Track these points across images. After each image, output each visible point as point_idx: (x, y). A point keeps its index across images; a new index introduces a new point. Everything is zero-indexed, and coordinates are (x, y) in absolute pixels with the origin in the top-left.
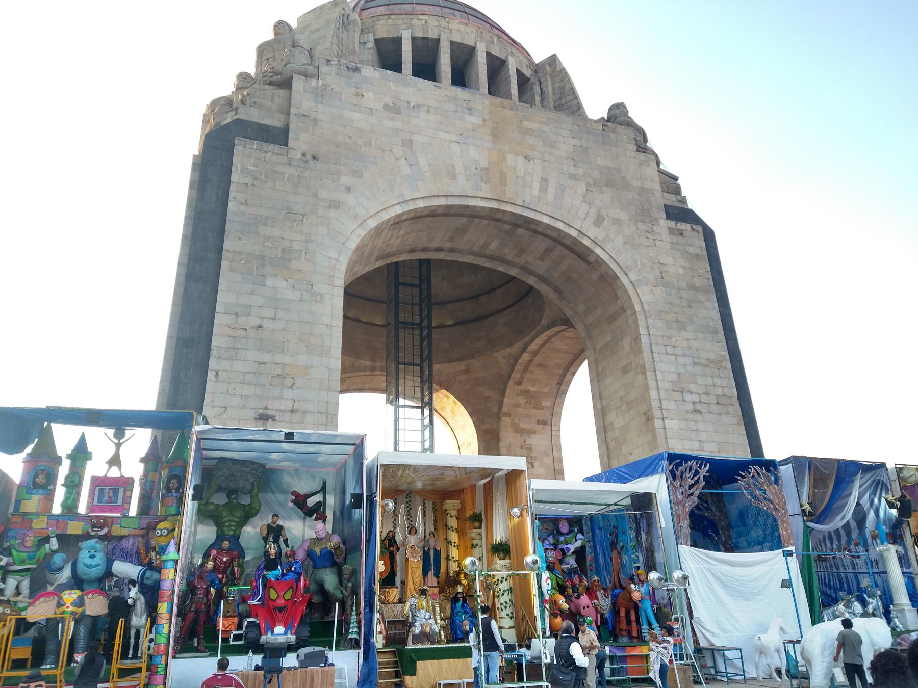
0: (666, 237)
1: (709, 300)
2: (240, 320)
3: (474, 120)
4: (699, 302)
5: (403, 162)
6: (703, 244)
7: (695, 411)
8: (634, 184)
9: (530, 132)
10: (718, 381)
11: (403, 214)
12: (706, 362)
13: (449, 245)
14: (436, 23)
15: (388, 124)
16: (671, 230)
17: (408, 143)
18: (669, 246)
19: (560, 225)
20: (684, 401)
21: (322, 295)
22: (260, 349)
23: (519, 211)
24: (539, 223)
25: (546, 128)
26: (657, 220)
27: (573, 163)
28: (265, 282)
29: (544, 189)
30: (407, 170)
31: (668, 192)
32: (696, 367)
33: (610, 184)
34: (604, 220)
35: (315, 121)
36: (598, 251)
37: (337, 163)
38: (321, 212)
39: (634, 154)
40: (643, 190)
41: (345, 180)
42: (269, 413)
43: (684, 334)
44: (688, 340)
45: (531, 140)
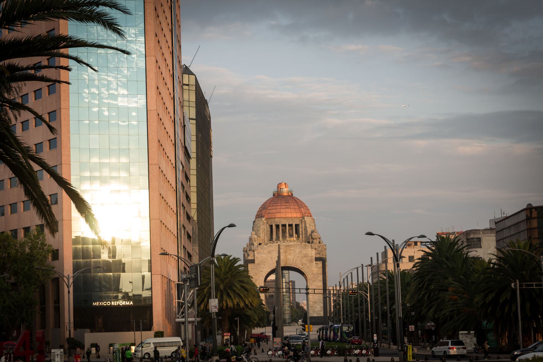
4: (319, 276)
5: (271, 262)
6: (322, 265)
9: (291, 250)
14: (279, 221)
15: (268, 255)
16: (316, 264)
17: (271, 258)
18: (315, 267)
19: (296, 267)
25: (294, 248)
26: (313, 262)
29: (293, 261)
30: (271, 263)
33: (305, 257)
35: (258, 258)
36: (302, 270)
37: (261, 264)
38: (260, 273)
40: (312, 257)
41: (263, 267)
43: (315, 282)
45: (291, 252)
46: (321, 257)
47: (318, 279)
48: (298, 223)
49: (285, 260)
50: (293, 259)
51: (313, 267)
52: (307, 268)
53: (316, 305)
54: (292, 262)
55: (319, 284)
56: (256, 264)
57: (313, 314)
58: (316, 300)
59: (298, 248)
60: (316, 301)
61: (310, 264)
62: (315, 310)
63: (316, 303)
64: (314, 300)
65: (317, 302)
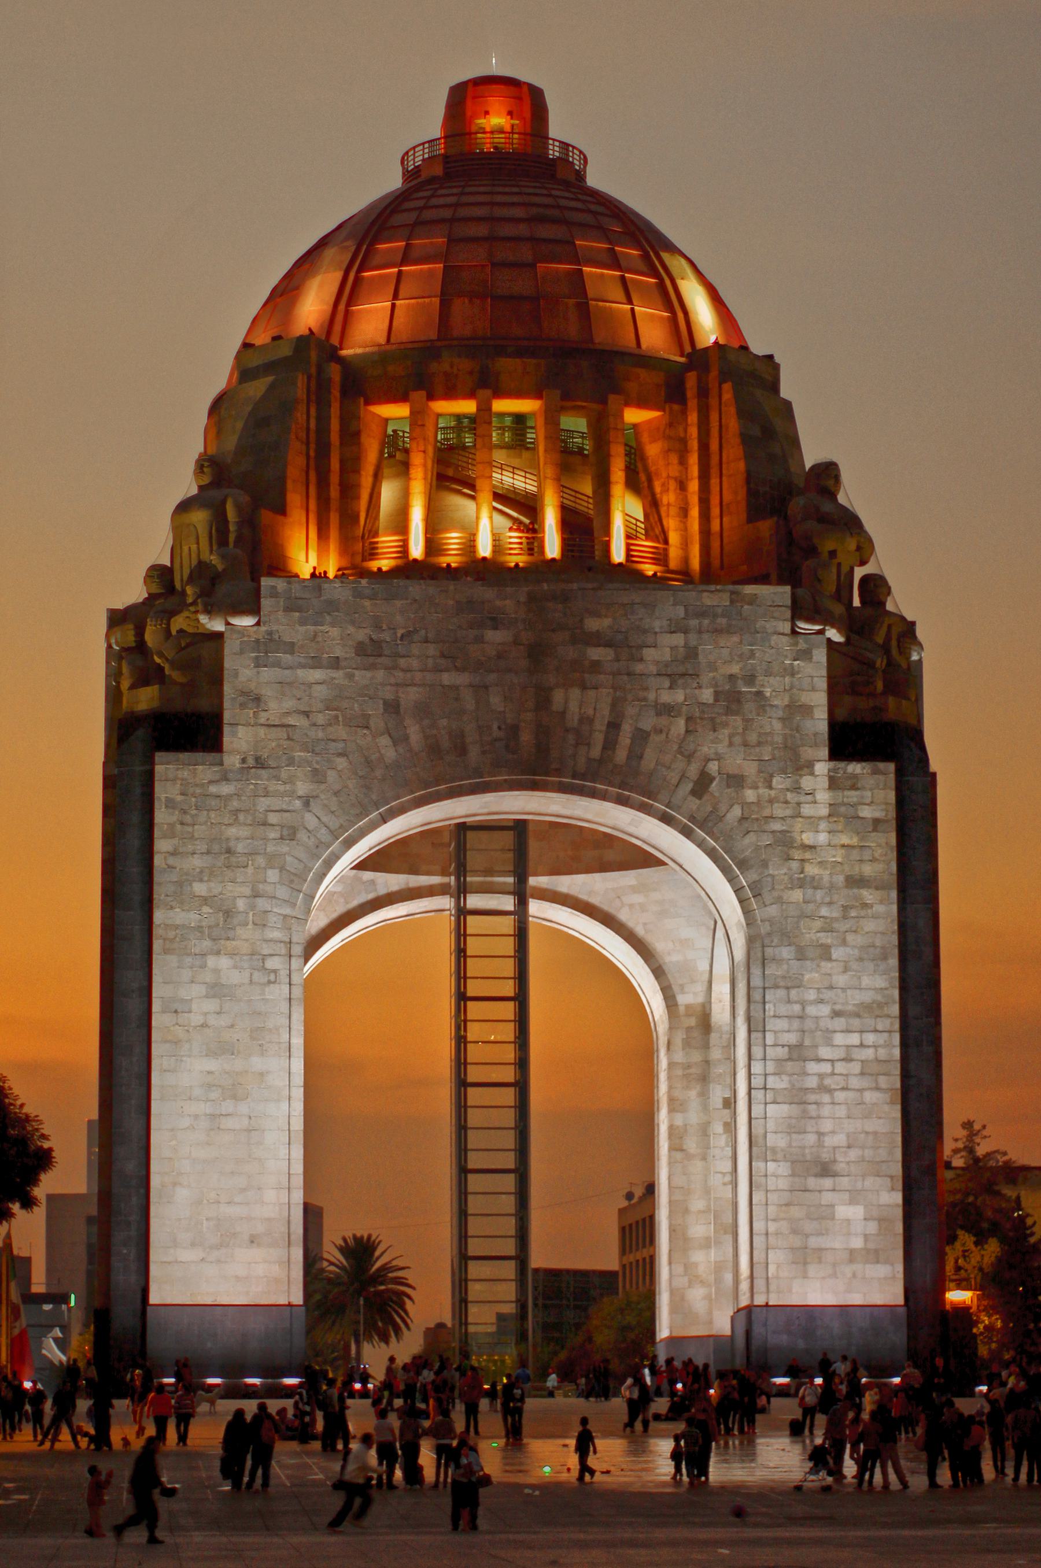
0: (823, 796)
1: (881, 902)
4: (865, 906)
6: (892, 796)
7: (823, 1089)
8: (776, 703)
9: (596, 639)
10: (870, 1038)
13: (485, 811)
16: (834, 784)
18: (824, 811)
20: (805, 1074)
21: (275, 971)
22: (207, 1055)
26: (810, 765)
27: (667, 683)
28: (206, 962)
29: (610, 744)
32: (836, 1019)
34: (712, 779)
35: (258, 699)
43: (826, 966)
45: (595, 653)
47: (850, 937)
51: (807, 810)
52: (743, 819)
53: (827, 1198)
54: (601, 761)
56: (232, 760)
58: (829, 1141)
60: (825, 1156)
61: (778, 782)
62: (814, 1242)
63: (825, 1170)
64: (811, 1139)
65: (840, 1167)
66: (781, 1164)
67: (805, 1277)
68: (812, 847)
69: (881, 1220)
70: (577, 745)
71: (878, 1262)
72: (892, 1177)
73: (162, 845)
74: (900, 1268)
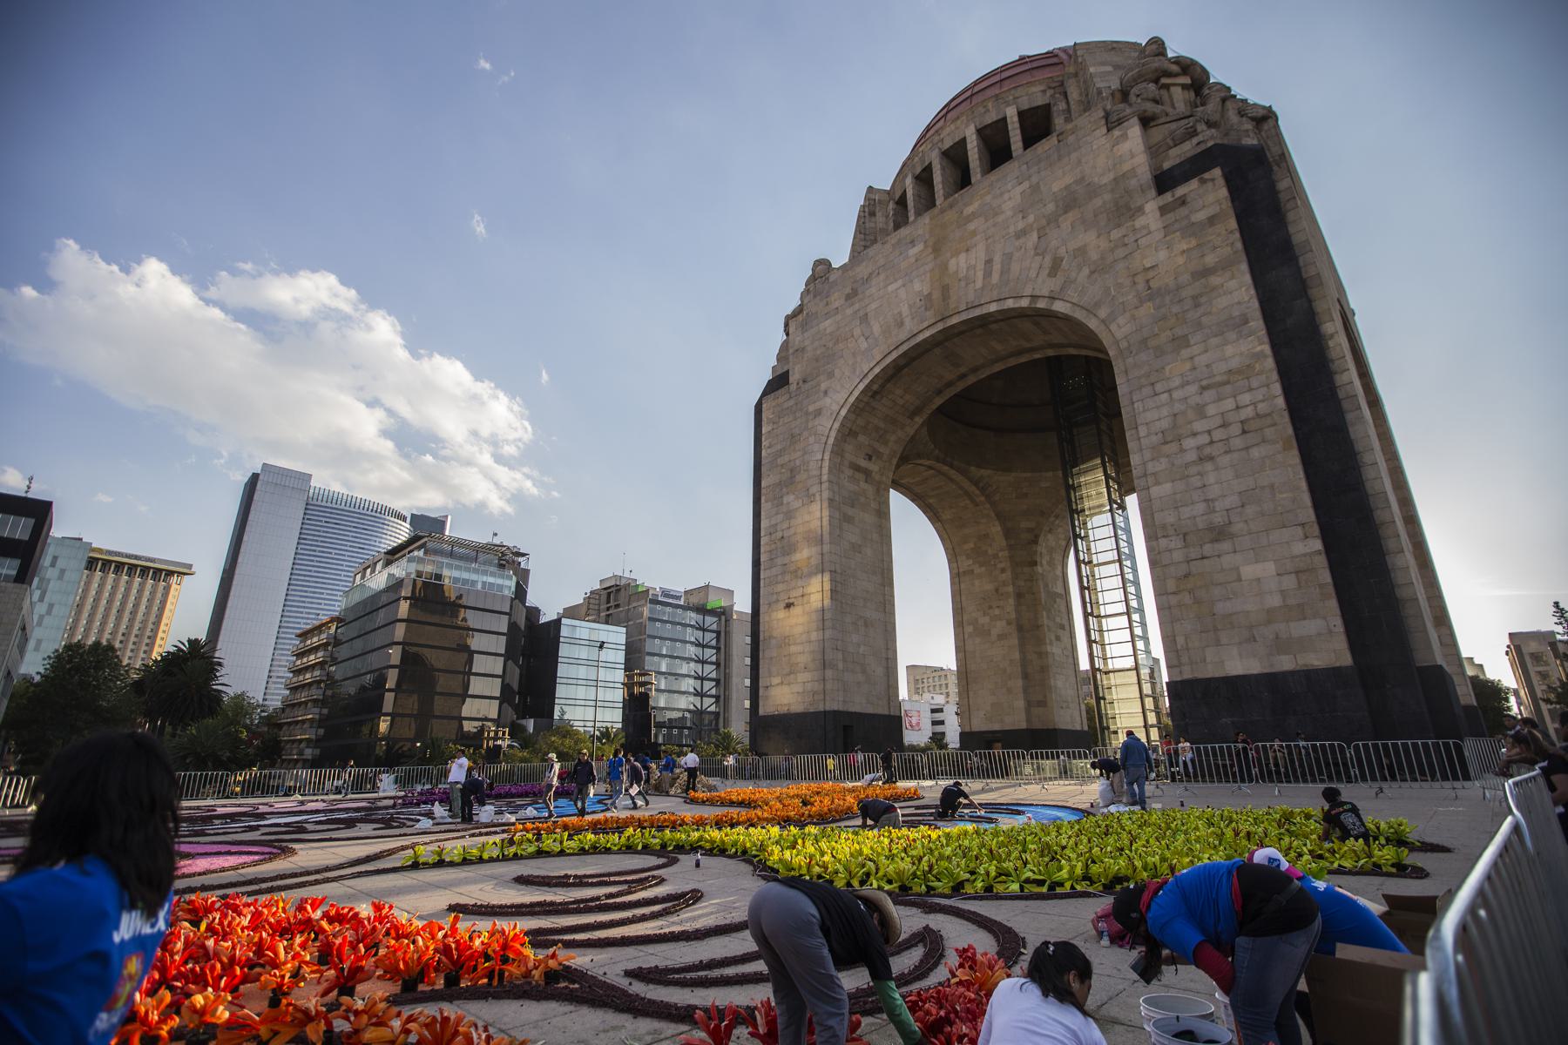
1: (1233, 277)
2: (773, 536)
3: (919, 247)
4: (1214, 289)
6: (1224, 192)
8: (1104, 182)
9: (973, 216)
10: (1246, 398)
11: (868, 387)
12: (1225, 378)
15: (849, 311)
16: (1163, 210)
19: (1010, 304)
20: (1182, 451)
23: (964, 317)
24: (990, 314)
25: (988, 198)
26: (1140, 210)
30: (864, 345)
31: (1175, 146)
35: (803, 349)
36: (1059, 307)
38: (810, 425)
39: (1103, 140)
41: (823, 386)
42: (791, 601)
43: (1185, 353)
44: (1192, 358)
45: (971, 226)
46: (1210, 144)
47: (1204, 319)
48: (1040, 101)
49: (936, 295)
50: (989, 262)
51: (1142, 242)
52: (1092, 272)
53: (1227, 560)
54: (983, 288)
55: (1229, 350)
56: (793, 387)
57: (1210, 654)
59: (1009, 186)
60: (1218, 519)
61: (1115, 234)
62: (1221, 608)
63: (1219, 533)
64: (1200, 508)
65: (1238, 527)
66: (1173, 538)
67: (1218, 643)
68: (1152, 267)
69: (1297, 573)
70: (967, 285)
71: (1305, 619)
72: (1303, 525)
73: (765, 443)
74: (1337, 623)
